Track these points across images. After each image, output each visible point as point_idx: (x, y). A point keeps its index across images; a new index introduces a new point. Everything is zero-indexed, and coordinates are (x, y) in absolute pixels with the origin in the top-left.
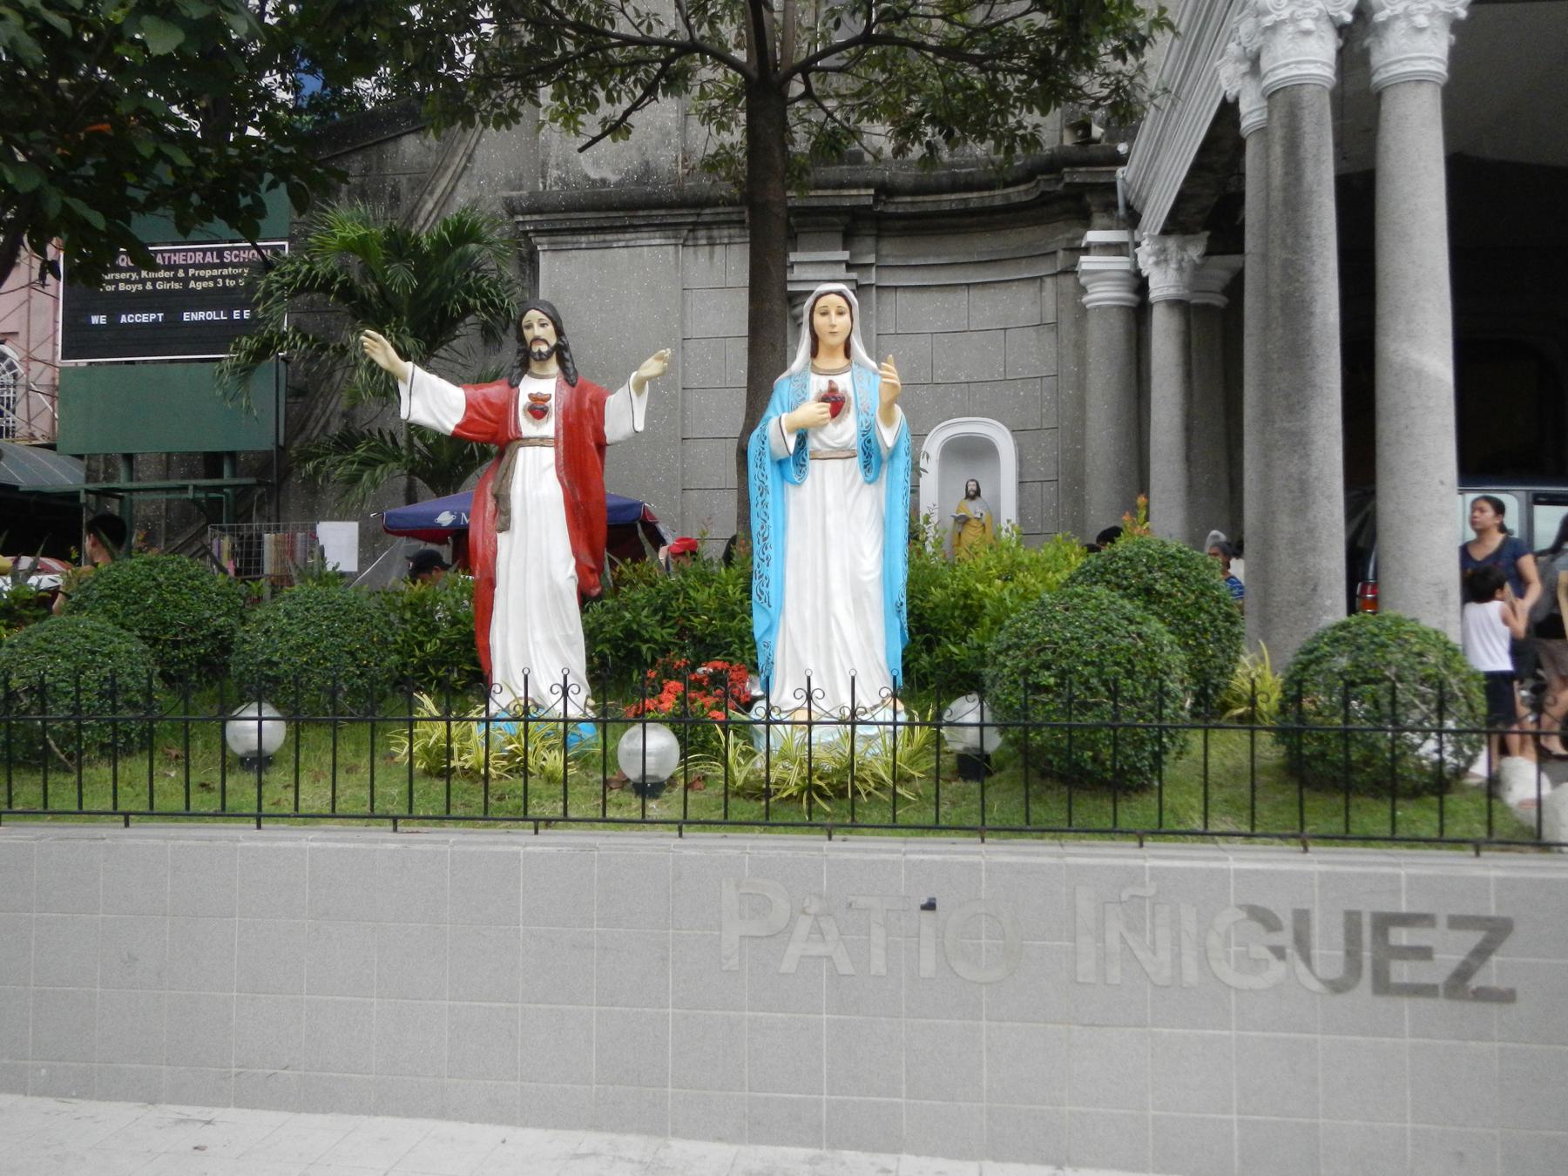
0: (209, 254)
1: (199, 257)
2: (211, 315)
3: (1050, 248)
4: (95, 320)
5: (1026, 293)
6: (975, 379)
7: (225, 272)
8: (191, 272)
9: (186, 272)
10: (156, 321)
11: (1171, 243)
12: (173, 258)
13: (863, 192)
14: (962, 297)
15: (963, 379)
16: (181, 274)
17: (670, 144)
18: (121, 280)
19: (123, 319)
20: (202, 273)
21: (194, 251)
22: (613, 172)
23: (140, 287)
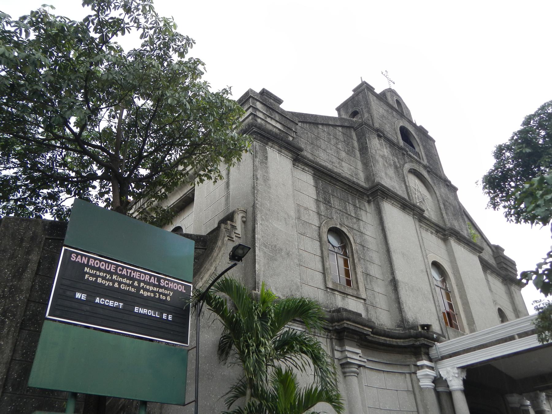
0: (153, 278)
1: (147, 278)
2: (151, 313)
3: (408, 363)
4: (78, 295)
5: (401, 377)
6: (391, 409)
7: (161, 291)
8: (142, 284)
9: (139, 284)
10: (117, 308)
11: (460, 370)
12: (132, 274)
13: (369, 330)
14: (382, 375)
15: (388, 408)
16: (136, 284)
17: (299, 291)
18: (99, 276)
19: (97, 300)
20: (148, 287)
21: (145, 274)
22: (282, 295)
23: (111, 284)
